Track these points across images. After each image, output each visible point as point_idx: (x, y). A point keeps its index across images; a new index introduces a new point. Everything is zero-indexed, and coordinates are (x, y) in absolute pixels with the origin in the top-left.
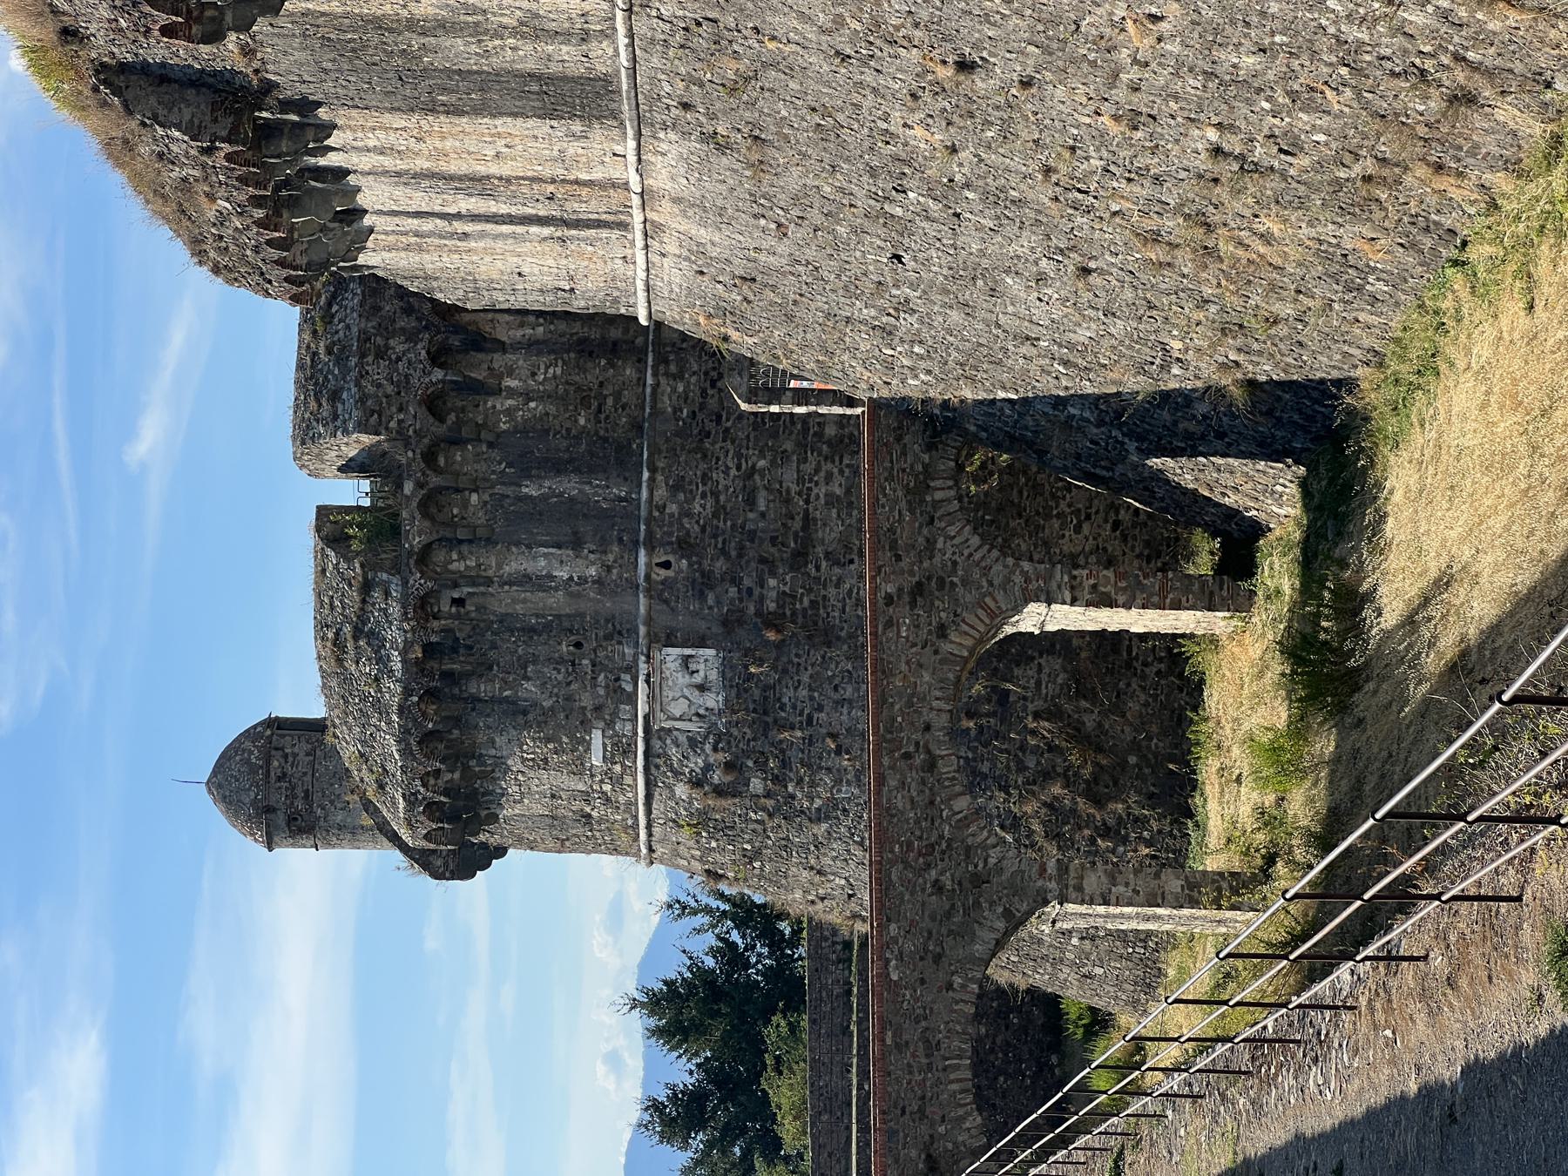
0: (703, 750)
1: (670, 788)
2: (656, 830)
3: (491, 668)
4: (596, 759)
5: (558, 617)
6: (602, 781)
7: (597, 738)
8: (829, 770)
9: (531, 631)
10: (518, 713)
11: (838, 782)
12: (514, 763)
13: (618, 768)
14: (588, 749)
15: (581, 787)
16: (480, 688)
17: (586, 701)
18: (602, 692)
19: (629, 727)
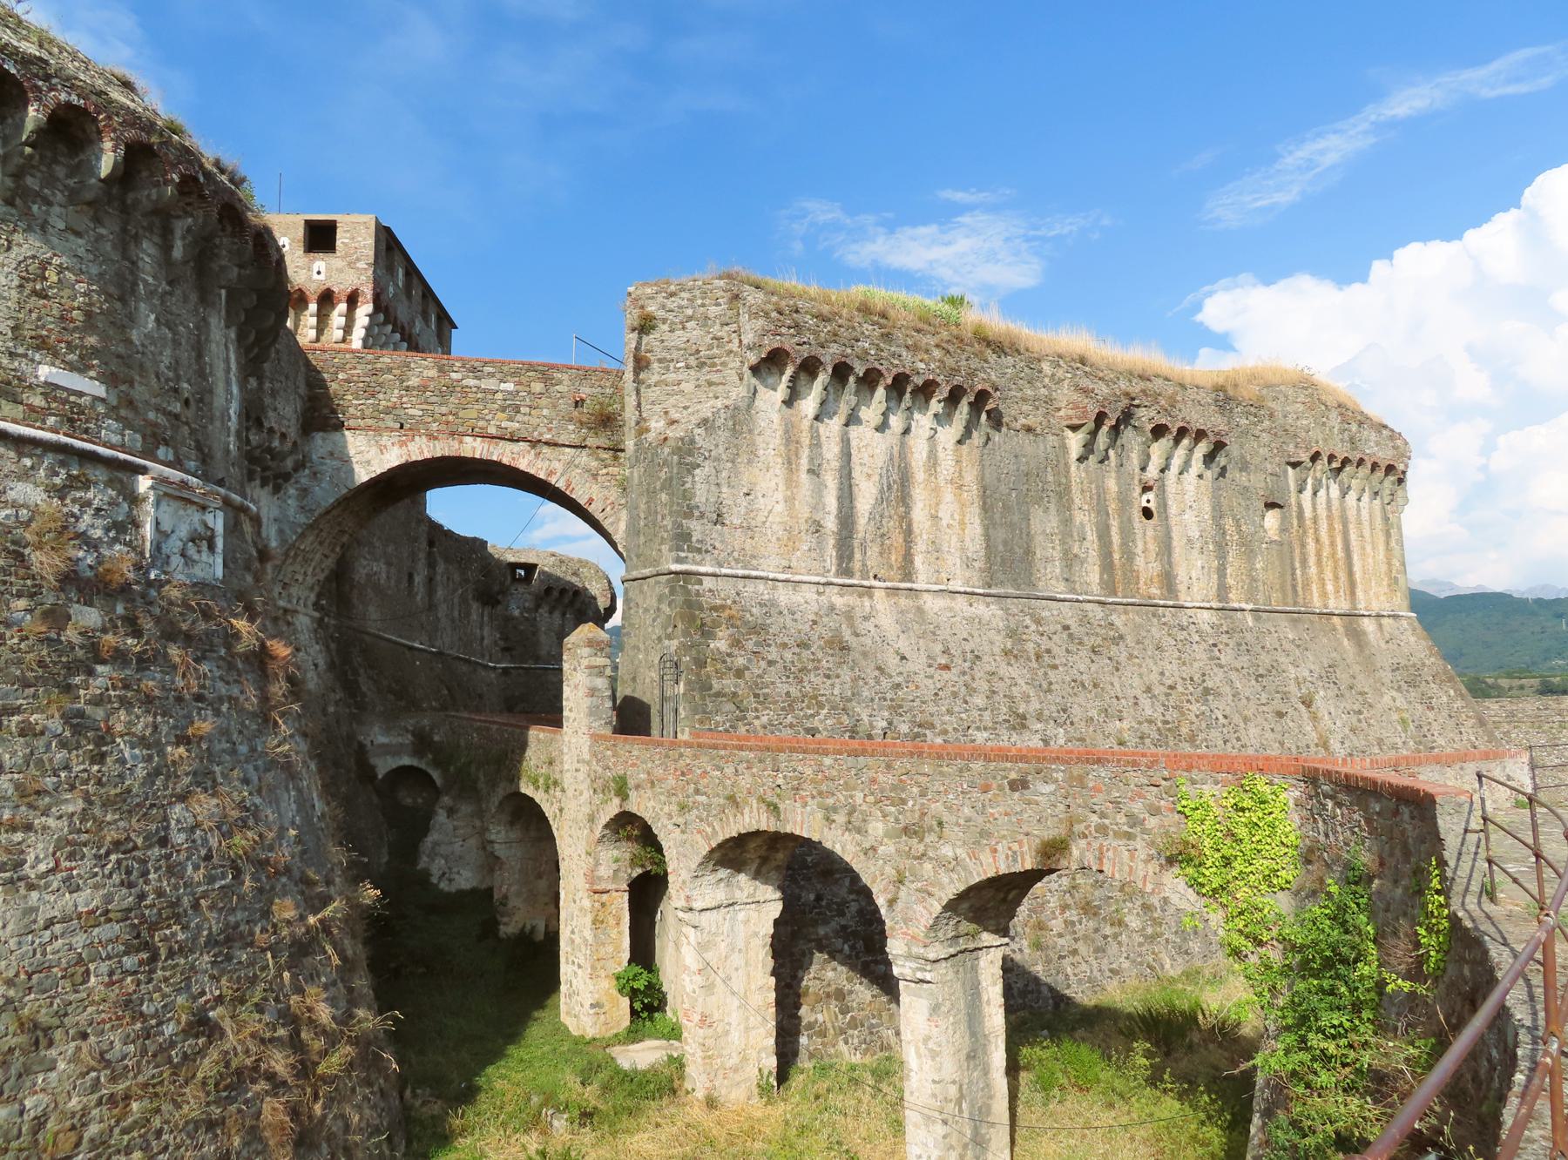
0: (115, 540)
1: (25, 475)
3: (170, 283)
4: (46, 372)
5: (211, 392)
7: (90, 386)
8: (155, 727)
9: (200, 356)
10: (121, 289)
11: (142, 742)
13: (38, 401)
14: (72, 367)
16: (147, 253)
18: (151, 415)
19: (115, 439)
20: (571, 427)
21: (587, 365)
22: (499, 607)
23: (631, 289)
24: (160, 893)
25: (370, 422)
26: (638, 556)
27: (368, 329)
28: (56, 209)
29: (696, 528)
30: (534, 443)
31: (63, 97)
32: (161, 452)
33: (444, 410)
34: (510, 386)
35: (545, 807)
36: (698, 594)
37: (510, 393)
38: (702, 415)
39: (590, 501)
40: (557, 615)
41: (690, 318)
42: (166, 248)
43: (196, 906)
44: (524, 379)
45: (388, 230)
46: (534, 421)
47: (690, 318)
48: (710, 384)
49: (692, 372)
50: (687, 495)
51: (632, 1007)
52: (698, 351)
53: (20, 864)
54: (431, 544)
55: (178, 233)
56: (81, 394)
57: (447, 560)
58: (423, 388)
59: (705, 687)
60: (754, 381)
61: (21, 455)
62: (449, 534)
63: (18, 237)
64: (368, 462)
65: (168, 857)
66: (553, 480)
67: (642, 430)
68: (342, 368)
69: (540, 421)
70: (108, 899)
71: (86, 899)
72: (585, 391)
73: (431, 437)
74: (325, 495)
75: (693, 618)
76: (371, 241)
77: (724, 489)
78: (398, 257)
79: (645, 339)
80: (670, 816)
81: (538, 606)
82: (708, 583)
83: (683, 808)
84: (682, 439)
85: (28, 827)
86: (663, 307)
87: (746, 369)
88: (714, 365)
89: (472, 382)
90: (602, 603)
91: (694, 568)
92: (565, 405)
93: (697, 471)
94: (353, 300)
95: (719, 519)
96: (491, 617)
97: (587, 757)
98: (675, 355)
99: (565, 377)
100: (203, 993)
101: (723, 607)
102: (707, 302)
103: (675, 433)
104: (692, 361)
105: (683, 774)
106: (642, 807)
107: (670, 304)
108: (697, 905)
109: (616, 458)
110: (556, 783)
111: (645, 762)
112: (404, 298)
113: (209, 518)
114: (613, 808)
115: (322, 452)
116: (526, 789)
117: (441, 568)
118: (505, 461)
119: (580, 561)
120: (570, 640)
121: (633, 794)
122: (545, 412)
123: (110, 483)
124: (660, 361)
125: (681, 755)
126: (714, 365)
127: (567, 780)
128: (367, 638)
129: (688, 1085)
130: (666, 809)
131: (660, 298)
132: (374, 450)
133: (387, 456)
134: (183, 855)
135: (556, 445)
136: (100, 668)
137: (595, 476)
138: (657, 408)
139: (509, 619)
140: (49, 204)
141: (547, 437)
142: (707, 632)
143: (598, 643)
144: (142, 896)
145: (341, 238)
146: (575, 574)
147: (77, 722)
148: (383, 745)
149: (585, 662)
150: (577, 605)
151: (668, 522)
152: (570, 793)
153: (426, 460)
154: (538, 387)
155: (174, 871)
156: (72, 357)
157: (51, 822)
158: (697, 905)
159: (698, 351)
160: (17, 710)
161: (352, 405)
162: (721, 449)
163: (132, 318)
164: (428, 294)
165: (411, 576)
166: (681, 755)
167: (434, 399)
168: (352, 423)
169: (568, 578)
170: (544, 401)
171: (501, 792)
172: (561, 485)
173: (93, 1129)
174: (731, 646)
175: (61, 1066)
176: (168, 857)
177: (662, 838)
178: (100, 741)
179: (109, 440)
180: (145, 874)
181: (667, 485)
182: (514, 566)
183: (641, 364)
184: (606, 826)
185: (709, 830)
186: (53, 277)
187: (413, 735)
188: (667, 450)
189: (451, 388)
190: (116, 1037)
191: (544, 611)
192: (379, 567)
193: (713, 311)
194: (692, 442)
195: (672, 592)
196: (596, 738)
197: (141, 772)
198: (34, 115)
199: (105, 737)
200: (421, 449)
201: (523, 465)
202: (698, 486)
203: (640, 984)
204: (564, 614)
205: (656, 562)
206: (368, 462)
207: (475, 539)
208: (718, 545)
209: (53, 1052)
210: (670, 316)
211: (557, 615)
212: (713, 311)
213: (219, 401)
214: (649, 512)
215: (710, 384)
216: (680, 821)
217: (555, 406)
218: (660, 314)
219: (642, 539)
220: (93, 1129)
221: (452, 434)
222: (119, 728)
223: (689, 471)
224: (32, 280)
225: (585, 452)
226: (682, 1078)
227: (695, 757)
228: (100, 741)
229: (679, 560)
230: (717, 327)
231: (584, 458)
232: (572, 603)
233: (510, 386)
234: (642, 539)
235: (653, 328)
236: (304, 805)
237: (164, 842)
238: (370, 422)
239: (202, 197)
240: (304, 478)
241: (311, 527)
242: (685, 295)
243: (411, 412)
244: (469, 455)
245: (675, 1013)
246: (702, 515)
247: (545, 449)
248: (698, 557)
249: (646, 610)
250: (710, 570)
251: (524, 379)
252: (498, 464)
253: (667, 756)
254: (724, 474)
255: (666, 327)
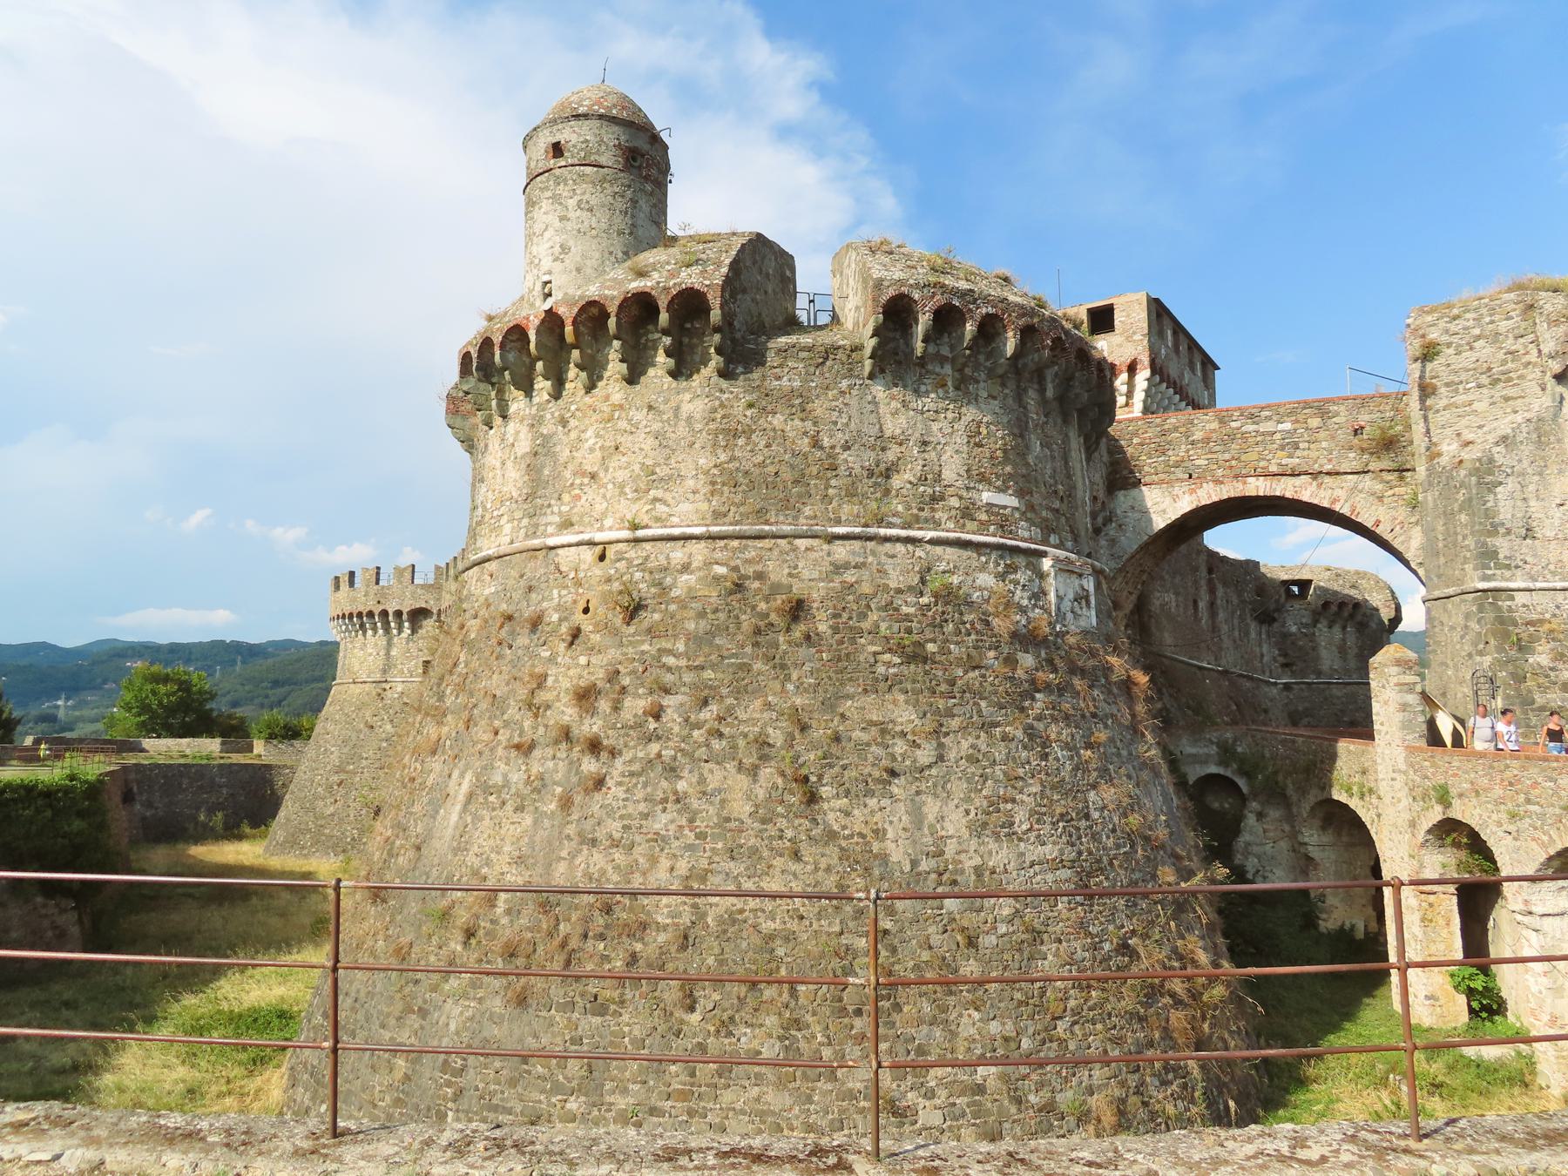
0: (1035, 606)
1: (983, 568)
2: (900, 547)
4: (987, 496)
5: (1075, 488)
6: (961, 498)
7: (1009, 500)
9: (1066, 463)
10: (1020, 429)
12: (970, 413)
13: (984, 517)
15: (948, 475)
16: (1032, 398)
17: (1036, 499)
18: (1044, 513)
19: (1026, 534)
20: (1352, 455)
21: (1364, 393)
22: (1276, 625)
23: (1409, 321)
24: (1090, 853)
25: (1162, 476)
26: (1439, 576)
27: (1147, 392)
28: (982, 384)
29: (1502, 545)
30: (1315, 475)
31: (984, 311)
32: (1053, 539)
33: (1227, 456)
34: (1287, 426)
35: (1361, 813)
36: (1510, 609)
37: (1288, 432)
38: (1503, 433)
39: (1377, 523)
40: (1337, 629)
41: (1478, 338)
42: (1042, 391)
43: (1111, 864)
44: (1301, 417)
45: (1157, 301)
46: (1314, 454)
47: (1478, 338)
48: (1507, 399)
49: (1485, 391)
50: (1489, 514)
51: (1469, 1006)
52: (1489, 369)
53: (1012, 824)
54: (1210, 571)
55: (1049, 379)
56: (1005, 507)
57: (1225, 584)
58: (1207, 440)
59: (1528, 702)
60: (1560, 389)
61: (980, 555)
62: (1225, 559)
63: (964, 410)
64: (1164, 511)
65: (1091, 827)
66: (1337, 508)
67: (1433, 454)
68: (1136, 434)
69: (1319, 454)
70: (1062, 852)
71: (1050, 851)
72: (1364, 418)
73: (1218, 482)
74: (1130, 543)
75: (1507, 635)
76: (1144, 315)
77: (1532, 503)
78: (1166, 321)
79: (1429, 366)
80: (1499, 824)
81: (1315, 622)
82: (1520, 598)
83: (1513, 816)
84: (1479, 460)
85: (1013, 801)
86: (1447, 331)
87: (1548, 378)
88: (1510, 379)
89: (1251, 428)
90: (1386, 614)
91: (1504, 585)
92: (1344, 435)
93: (1499, 489)
94: (1132, 369)
95: (1529, 533)
96: (1268, 636)
97: (1403, 767)
98: (1463, 376)
99: (1342, 408)
100: (1123, 926)
101: (1541, 622)
102: (1497, 317)
103: (1469, 455)
104: (1484, 380)
105: (1511, 784)
106: (1467, 815)
107: (1453, 327)
108: (1538, 910)
109: (1402, 478)
110: (1371, 791)
111: (1467, 772)
112: (1173, 355)
113: (1085, 583)
114: (1436, 814)
115: (1125, 506)
116: (1338, 795)
117: (1220, 592)
118: (1288, 495)
119: (1357, 573)
120: (1376, 660)
121: (1456, 803)
122: (1324, 444)
123: (1027, 567)
124: (1447, 385)
125: (1507, 767)
126: (1510, 379)
127: (1383, 788)
128: (1166, 662)
129: (1541, 1081)
130: (1495, 817)
131: (1442, 324)
132: (1168, 500)
133: (1179, 504)
134: (1100, 827)
135: (1338, 474)
136: (1038, 696)
137: (1380, 498)
138: (1448, 431)
139: (1286, 635)
140: (977, 382)
141: (1328, 467)
142: (1523, 648)
143: (1406, 662)
144: (1080, 853)
145: (1119, 318)
146: (1353, 587)
147: (1030, 731)
148: (1190, 755)
149: (1395, 680)
150: (1359, 618)
151: (1470, 542)
152: (1387, 800)
153: (1215, 504)
154: (1315, 422)
155: (1095, 837)
156: (999, 483)
157: (1025, 798)
158: (1538, 910)
159: (1489, 369)
160: (997, 725)
161: (1147, 464)
162: (1525, 463)
163: (1027, 447)
164: (1193, 345)
165: (1195, 602)
166: (1507, 767)
167: (1218, 448)
168: (1147, 479)
169: (1346, 591)
170: (1322, 434)
171: (1313, 797)
172: (1346, 511)
173: (1072, 1003)
174: (1555, 659)
175: (1050, 957)
176: (1091, 827)
177: (1491, 843)
178: (1044, 745)
179: (1024, 536)
180: (1079, 838)
181: (1467, 505)
182: (1287, 584)
183: (1426, 391)
184: (1429, 832)
185: (1545, 838)
186: (984, 431)
187: (1218, 745)
188: (1463, 473)
189: (1232, 437)
190: (1077, 945)
191: (1322, 625)
192: (1170, 598)
193: (1504, 325)
194: (1491, 461)
195: (1481, 610)
196: (1411, 750)
197: (1068, 768)
198: (970, 328)
199: (1046, 744)
200: (1209, 494)
201: (1306, 497)
202: (1502, 503)
203: (1478, 984)
204: (1344, 628)
205: (1460, 581)
206: (1164, 511)
207: (1248, 562)
208: (1529, 559)
209: (1044, 948)
210: (1455, 339)
211: (1337, 629)
212: (1504, 325)
213: (1080, 494)
214: (1447, 533)
215: (1507, 399)
216: (1511, 828)
217: (1333, 438)
218: (1445, 338)
219: (1442, 560)
220: (1072, 1003)
221: (1236, 477)
222: (1053, 736)
223: (1490, 491)
224: (973, 435)
225: (1368, 477)
226: (1533, 1073)
227: (1524, 768)
228: (1044, 745)
229: (1485, 578)
230: (1511, 340)
231: (1367, 482)
232: (1352, 616)
233: (1287, 426)
234: (1442, 560)
235: (1437, 354)
236: (1165, 794)
237: (1087, 817)
238: (1162, 476)
239: (1064, 350)
240: (1112, 529)
241: (1120, 570)
242: (1468, 316)
243: (1197, 462)
244: (1254, 494)
245: (1518, 1018)
246: (1509, 531)
247: (1327, 479)
248: (1507, 574)
249: (1452, 628)
250: (1522, 585)
251: (1301, 417)
252: (1282, 498)
253: (1491, 767)
254: (1532, 488)
255: (1451, 351)
